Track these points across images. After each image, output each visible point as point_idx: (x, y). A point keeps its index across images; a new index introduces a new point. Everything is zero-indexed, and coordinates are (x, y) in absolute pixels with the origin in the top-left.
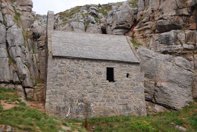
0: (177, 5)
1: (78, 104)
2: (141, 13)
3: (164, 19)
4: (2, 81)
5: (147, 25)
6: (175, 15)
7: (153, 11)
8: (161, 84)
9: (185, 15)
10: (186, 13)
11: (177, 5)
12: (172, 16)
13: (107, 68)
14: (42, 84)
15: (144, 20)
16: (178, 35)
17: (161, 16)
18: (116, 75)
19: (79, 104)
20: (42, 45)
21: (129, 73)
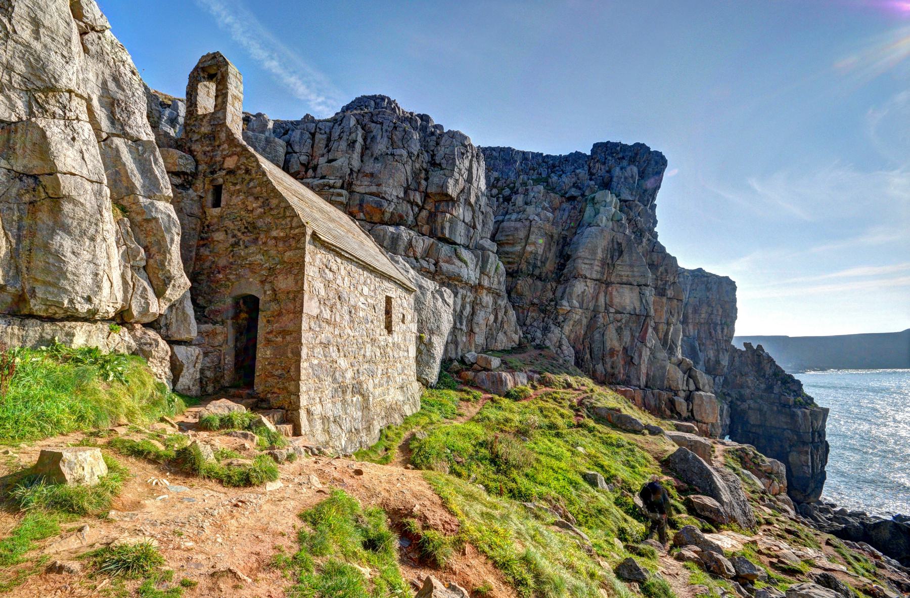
0: (407, 180)
1: (352, 401)
2: (303, 158)
3: (383, 198)
4: (83, 308)
5: (340, 195)
6: (402, 198)
7: (351, 170)
8: (430, 339)
9: (417, 205)
10: (420, 203)
11: (407, 180)
12: (397, 197)
13: (387, 297)
14: (219, 328)
15: (332, 182)
16: (414, 240)
17: (374, 189)
18: (396, 317)
19: (355, 399)
20: (188, 171)
21: (405, 313)
